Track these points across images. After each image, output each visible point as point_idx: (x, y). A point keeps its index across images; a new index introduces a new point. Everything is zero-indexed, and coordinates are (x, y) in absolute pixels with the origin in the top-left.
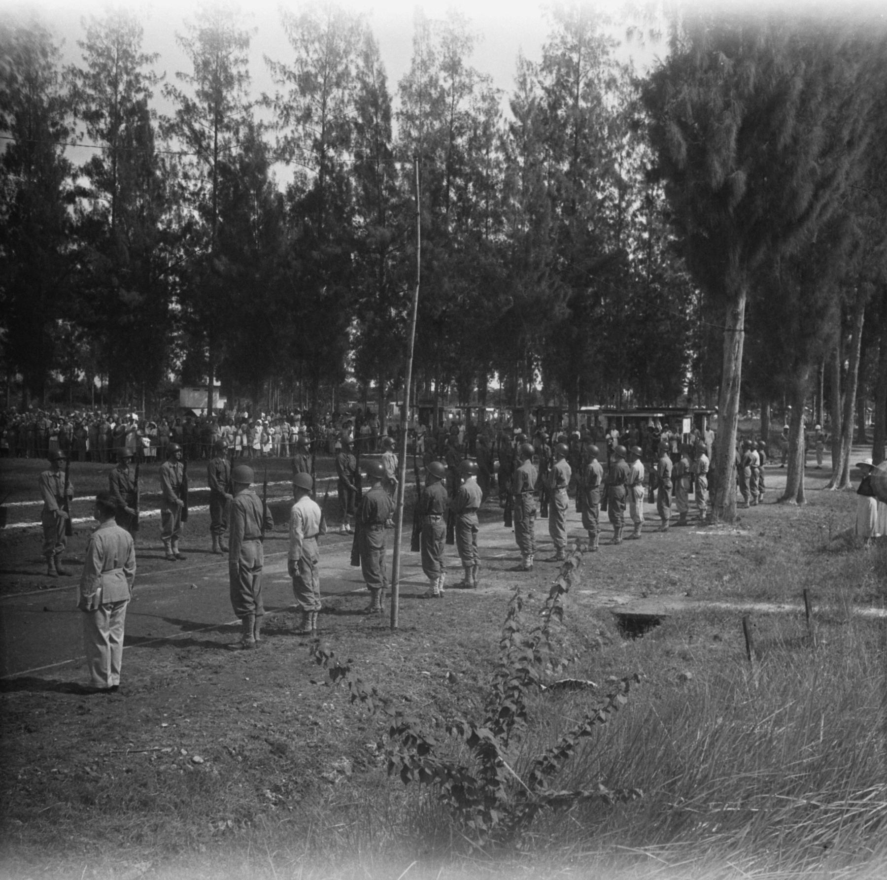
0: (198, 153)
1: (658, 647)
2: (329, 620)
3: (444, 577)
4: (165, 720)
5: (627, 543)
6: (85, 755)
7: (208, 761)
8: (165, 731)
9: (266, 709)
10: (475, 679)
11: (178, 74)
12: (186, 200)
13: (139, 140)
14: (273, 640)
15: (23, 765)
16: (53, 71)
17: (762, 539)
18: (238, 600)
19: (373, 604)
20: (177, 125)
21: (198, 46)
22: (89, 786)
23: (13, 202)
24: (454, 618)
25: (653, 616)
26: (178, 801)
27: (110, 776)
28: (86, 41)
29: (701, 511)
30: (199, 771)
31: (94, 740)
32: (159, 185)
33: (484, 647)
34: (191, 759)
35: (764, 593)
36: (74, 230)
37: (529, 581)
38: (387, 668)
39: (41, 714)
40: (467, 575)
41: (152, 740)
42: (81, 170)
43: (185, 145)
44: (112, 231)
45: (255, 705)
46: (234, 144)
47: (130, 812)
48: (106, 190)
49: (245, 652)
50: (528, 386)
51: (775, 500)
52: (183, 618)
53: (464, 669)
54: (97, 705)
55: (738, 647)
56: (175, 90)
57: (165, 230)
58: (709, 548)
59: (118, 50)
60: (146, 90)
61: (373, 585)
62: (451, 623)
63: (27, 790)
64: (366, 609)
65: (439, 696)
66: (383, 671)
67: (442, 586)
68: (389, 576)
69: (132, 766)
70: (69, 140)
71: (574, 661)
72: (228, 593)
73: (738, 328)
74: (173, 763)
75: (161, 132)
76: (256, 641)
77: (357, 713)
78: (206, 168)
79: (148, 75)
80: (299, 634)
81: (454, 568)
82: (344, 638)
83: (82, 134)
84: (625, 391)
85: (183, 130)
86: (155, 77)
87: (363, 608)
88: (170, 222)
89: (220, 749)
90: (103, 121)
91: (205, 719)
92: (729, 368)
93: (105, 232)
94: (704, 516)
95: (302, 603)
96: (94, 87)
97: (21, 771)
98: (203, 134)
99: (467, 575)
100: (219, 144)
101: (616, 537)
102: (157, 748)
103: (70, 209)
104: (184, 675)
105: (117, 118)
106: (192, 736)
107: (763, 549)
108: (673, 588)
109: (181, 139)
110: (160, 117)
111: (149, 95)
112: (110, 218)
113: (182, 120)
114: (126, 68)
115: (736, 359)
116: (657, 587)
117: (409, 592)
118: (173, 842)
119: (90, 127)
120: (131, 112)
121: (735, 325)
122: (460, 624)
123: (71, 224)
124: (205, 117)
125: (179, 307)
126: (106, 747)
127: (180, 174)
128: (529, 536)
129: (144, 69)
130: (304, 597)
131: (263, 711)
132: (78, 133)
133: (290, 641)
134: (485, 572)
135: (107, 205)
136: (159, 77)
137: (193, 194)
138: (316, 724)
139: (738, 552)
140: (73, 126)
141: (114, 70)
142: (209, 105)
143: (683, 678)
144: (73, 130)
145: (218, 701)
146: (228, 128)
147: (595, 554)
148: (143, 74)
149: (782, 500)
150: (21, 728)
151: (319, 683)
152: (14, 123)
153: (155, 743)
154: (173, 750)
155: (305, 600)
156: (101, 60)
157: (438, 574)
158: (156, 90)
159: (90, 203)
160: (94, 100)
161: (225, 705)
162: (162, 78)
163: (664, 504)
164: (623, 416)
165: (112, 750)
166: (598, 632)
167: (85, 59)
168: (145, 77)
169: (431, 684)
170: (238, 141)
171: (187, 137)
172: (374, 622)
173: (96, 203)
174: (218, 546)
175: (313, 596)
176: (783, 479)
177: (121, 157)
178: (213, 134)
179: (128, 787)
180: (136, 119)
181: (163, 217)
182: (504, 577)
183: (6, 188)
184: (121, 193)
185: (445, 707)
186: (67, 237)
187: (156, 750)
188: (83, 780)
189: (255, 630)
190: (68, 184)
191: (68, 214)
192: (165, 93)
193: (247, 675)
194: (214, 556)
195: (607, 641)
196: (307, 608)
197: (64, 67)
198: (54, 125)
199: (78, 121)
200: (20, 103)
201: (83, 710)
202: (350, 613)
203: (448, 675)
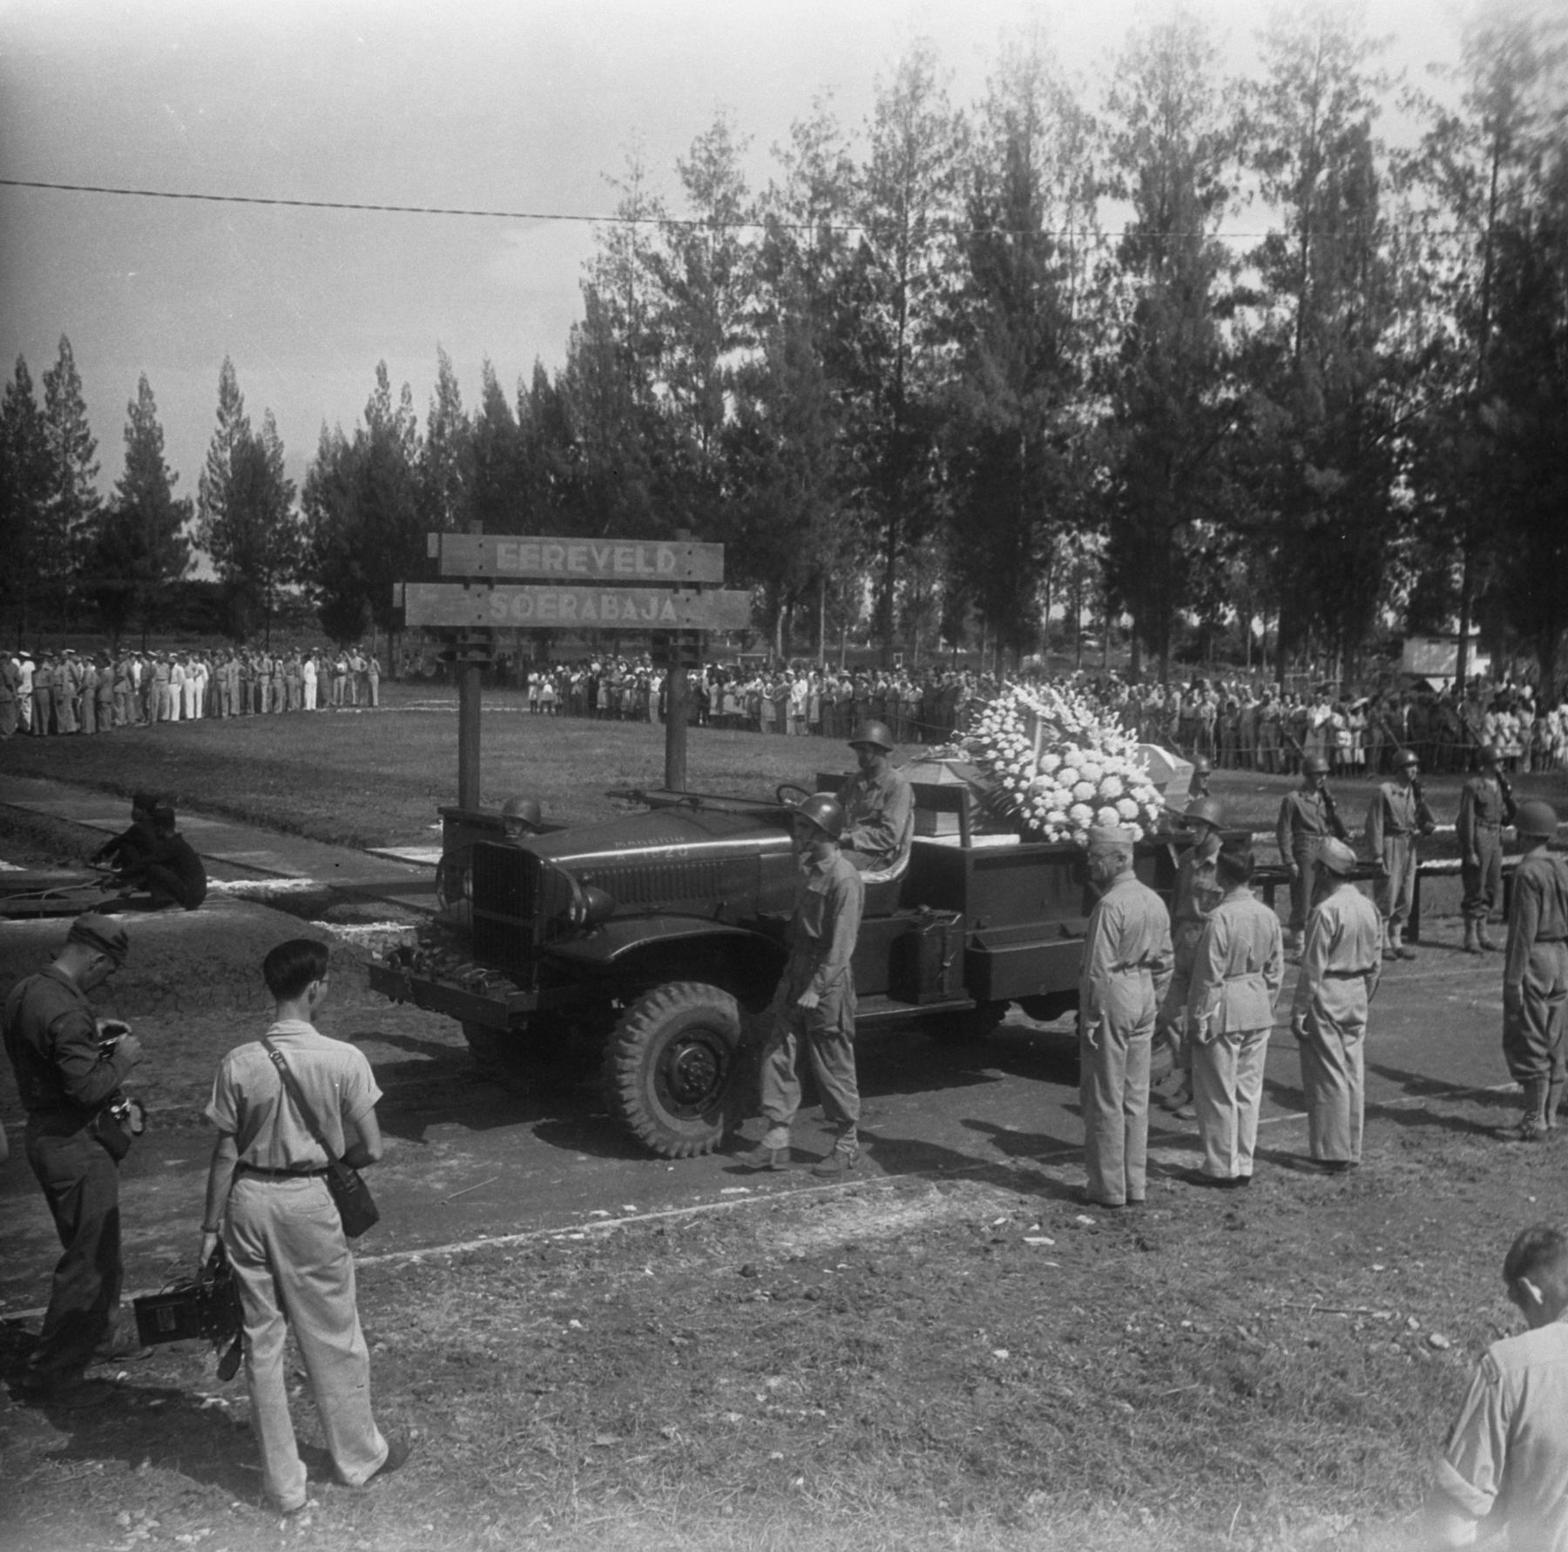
0: (1460, 210)
4: (1379, 1258)
6: (1237, 1305)
7: (1458, 1345)
8: (1378, 1280)
11: (1431, 67)
12: (1432, 299)
13: (1352, 196)
15: (1134, 1308)
16: (1206, 89)
18: (1515, 1045)
20: (1424, 162)
22: (1246, 1362)
23: (1130, 321)
26: (1403, 1412)
27: (1281, 1349)
30: (1442, 1364)
31: (1253, 1279)
32: (1383, 274)
34: (1428, 1339)
36: (1228, 364)
39: (1162, 1221)
41: (1356, 1293)
42: (1247, 258)
43: (1436, 197)
44: (1295, 363)
46: (1529, 187)
47: (1316, 1420)
48: (1287, 290)
49: (1528, 1146)
52: (1410, 1068)
56: (1422, 97)
57: (1391, 356)
60: (1369, 104)
63: (1141, 1354)
69: (1320, 1335)
70: (1228, 205)
72: (1499, 1028)
74: (1394, 1340)
75: (1391, 178)
76: (1550, 1129)
78: (1474, 238)
83: (1251, 193)
85: (1432, 171)
88: (1401, 342)
89: (1480, 1326)
90: (1287, 167)
91: (1453, 1266)
93: (1282, 366)
96: (1277, 109)
97: (1132, 1318)
98: (1470, 174)
100: (1500, 190)
102: (1363, 1308)
103: (1225, 327)
104: (1413, 1177)
105: (1313, 161)
106: (1428, 1296)
109: (1428, 187)
110: (1391, 151)
111: (1375, 112)
112: (1293, 340)
113: (1433, 154)
114: (1335, 68)
118: (1392, 1487)
119: (1266, 180)
120: (1341, 147)
123: (1225, 355)
124: (1476, 140)
125: (1410, 494)
126: (1274, 1295)
127: (1425, 252)
129: (1366, 68)
132: (1244, 193)
135: (1287, 315)
136: (1392, 78)
137: (1445, 286)
144: (1236, 189)
145: (1476, 1234)
146: (1519, 157)
148: (1364, 76)
150: (1129, 1241)
152: (1138, 186)
153: (1360, 1300)
154: (1394, 1316)
156: (1292, 60)
158: (1386, 101)
159: (1260, 316)
161: (1490, 1244)
162: (1399, 80)
165: (1284, 1302)
167: (1263, 59)
168: (1368, 81)
170: (1537, 180)
171: (1441, 183)
173: (1270, 315)
174: (1475, 941)
177: (1316, 229)
178: (1490, 172)
179: (1312, 1374)
180: (1348, 158)
181: (1389, 332)
183: (1119, 300)
184: (1314, 293)
186: (1218, 377)
187: (1363, 1313)
188: (1234, 1350)
189: (1548, 1106)
190: (1222, 285)
191: (1221, 337)
192: (1403, 103)
194: (1467, 956)
197: (1226, 79)
199: (1243, 172)
200: (1149, 152)
201: (1232, 1223)
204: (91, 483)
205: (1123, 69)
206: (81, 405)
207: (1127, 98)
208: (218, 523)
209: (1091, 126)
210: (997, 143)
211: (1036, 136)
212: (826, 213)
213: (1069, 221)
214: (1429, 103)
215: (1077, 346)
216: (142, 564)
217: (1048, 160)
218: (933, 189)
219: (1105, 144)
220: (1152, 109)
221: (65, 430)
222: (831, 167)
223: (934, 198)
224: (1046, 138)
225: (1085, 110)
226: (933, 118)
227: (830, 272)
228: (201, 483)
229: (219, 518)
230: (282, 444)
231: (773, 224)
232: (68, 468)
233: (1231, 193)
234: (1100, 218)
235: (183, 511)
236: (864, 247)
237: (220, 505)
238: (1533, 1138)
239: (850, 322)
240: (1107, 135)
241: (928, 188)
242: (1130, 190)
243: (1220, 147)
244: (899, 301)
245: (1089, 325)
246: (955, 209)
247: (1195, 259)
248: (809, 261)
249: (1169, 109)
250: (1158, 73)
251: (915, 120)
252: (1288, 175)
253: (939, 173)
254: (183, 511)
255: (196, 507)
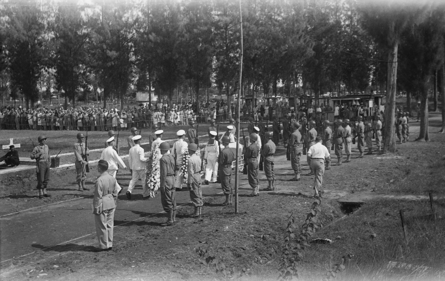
1: (360, 220)
2: (207, 209)
3: (259, 187)
5: (344, 165)
9: (179, 257)
10: (274, 238)
14: (182, 221)
17: (409, 160)
19: (227, 201)
24: (264, 206)
25: (357, 203)
29: (379, 147)
33: (278, 221)
35: (410, 190)
37: (299, 186)
38: (234, 234)
40: (270, 185)
45: (174, 255)
49: (169, 227)
50: (296, 85)
51: (414, 139)
53: (269, 233)
54: (102, 257)
55: (399, 220)
58: (383, 166)
61: (227, 193)
62: (262, 209)
64: (224, 203)
65: (258, 247)
66: (232, 235)
67: (258, 191)
68: (233, 187)
71: (320, 226)
73: (394, 61)
77: (221, 257)
80: (193, 217)
81: (263, 180)
82: (214, 218)
84: (341, 86)
87: (222, 203)
92: (390, 80)
94: (380, 149)
95: (194, 203)
99: (270, 185)
101: (339, 162)
104: (142, 240)
107: (409, 166)
108: (366, 188)
115: (394, 75)
116: (358, 187)
117: (243, 193)
121: (393, 59)
122: (267, 209)
128: (297, 165)
130: (195, 200)
131: (177, 258)
133: (190, 220)
134: (278, 182)
138: (202, 263)
139: (397, 167)
143: (372, 237)
147: (329, 171)
149: (417, 140)
151: (203, 242)
155: (195, 201)
157: (256, 185)
163: (361, 145)
164: (340, 100)
166: (331, 211)
169: (254, 241)
172: (227, 210)
175: (199, 199)
176: (418, 128)
182: (287, 184)
185: (261, 253)
193: (170, 239)
195: (336, 216)
196: (197, 205)
202: (217, 205)
203: (262, 236)
238: (170, 225)
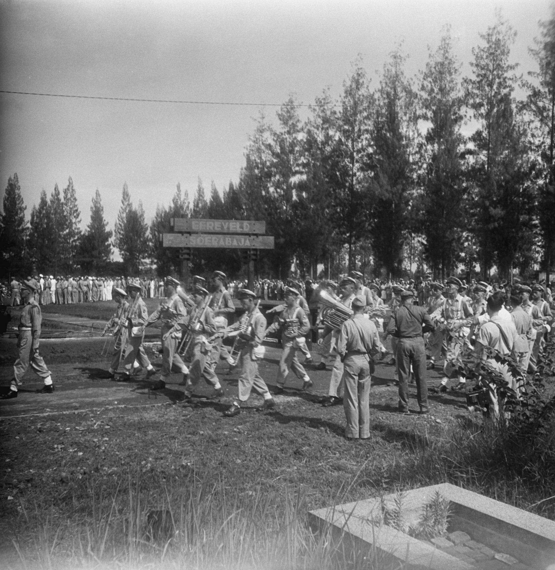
0: (541, 120)
11: (529, 73)
16: (454, 83)
21: (543, 53)
23: (430, 161)
28: (474, 62)
43: (533, 116)
48: (484, 149)
56: (528, 83)
59: (493, 65)
60: (510, 86)
70: (463, 122)
78: (547, 129)
79: (511, 77)
83: (471, 117)
85: (531, 107)
86: (516, 77)
90: (482, 108)
96: (478, 88)
109: (530, 113)
111: (512, 90)
112: (486, 166)
114: (498, 75)
119: (475, 113)
120: (501, 100)
124: (546, 97)
127: (529, 135)
129: (509, 74)
132: (468, 117)
136: (518, 78)
137: (537, 147)
140: (465, 114)
141: (491, 77)
142: (549, 90)
144: (465, 116)
148: (508, 77)
152: (432, 116)
159: (474, 157)
160: (478, 96)
167: (474, 72)
168: (510, 79)
171: (534, 111)
177: (493, 129)
178: (551, 107)
183: (426, 154)
190: (461, 148)
198: (455, 114)
199: (468, 110)
204: (79, 226)
205: (426, 76)
206: (75, 199)
207: (427, 86)
208: (121, 238)
209: (416, 96)
210: (384, 103)
211: (397, 100)
212: (327, 129)
213: (408, 128)
214: (530, 85)
215: (412, 170)
216: (95, 253)
217: (401, 108)
218: (364, 119)
219: (420, 102)
220: (436, 90)
221: (70, 208)
222: (328, 113)
223: (364, 122)
224: (401, 101)
225: (414, 91)
226: (363, 96)
227: (328, 149)
228: (115, 225)
229: (121, 236)
230: (144, 212)
231: (309, 132)
232: (71, 220)
233: (464, 117)
234: (419, 126)
235: (109, 234)
236: (340, 140)
237: (122, 232)
239: (335, 165)
240: (421, 99)
241: (362, 119)
242: (429, 117)
243: (461, 102)
244: (352, 158)
245: (415, 163)
246: (370, 125)
247: (452, 139)
248: (322, 145)
249: (441, 90)
250: (437, 77)
251: (357, 96)
252: (483, 110)
253: (365, 114)
254: (109, 234)
255: (114, 233)
